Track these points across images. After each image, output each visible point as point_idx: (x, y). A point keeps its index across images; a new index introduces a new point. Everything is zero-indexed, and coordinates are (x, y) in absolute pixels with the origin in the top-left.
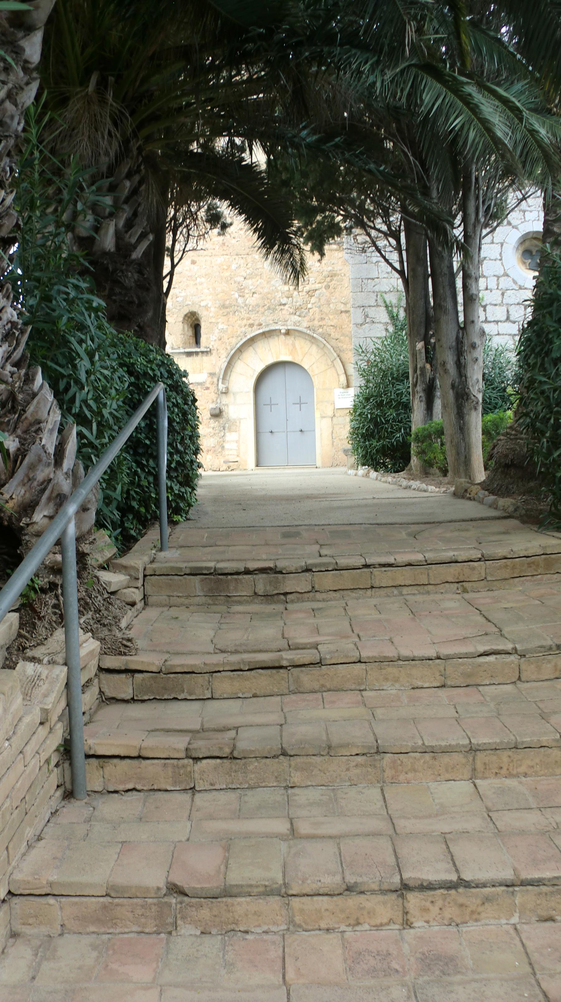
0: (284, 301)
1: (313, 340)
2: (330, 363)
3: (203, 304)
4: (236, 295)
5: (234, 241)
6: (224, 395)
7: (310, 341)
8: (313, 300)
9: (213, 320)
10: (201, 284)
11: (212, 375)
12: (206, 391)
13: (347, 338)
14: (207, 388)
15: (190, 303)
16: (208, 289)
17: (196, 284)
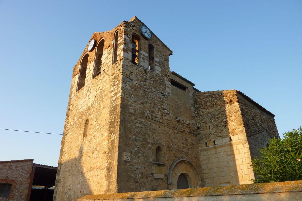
0: (183, 150)
1: (192, 165)
2: (195, 176)
3: (162, 144)
4: (171, 144)
5: (169, 123)
6: (169, 185)
7: (190, 167)
8: (189, 152)
9: (165, 152)
10: (162, 136)
11: (165, 175)
12: (164, 183)
13: (198, 168)
14: (164, 182)
15: (159, 143)
16: (164, 139)
17: (160, 136)
